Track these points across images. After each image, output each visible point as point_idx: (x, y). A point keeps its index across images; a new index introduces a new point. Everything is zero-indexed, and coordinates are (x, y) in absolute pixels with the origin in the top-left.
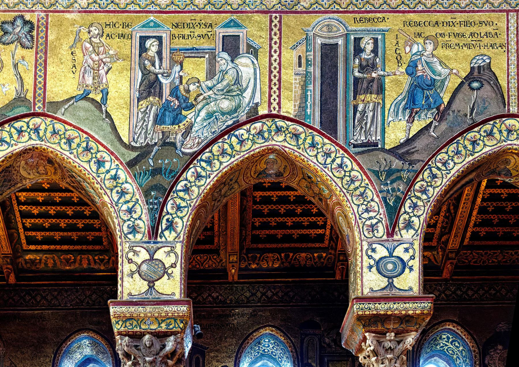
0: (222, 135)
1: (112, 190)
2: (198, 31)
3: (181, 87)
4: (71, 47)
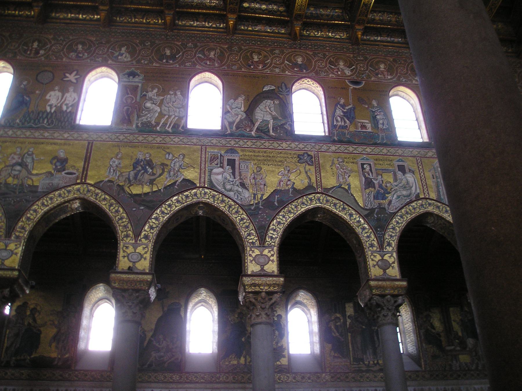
0: (405, 206)
1: (358, 227)
2: (386, 163)
3: (383, 185)
4: (331, 166)
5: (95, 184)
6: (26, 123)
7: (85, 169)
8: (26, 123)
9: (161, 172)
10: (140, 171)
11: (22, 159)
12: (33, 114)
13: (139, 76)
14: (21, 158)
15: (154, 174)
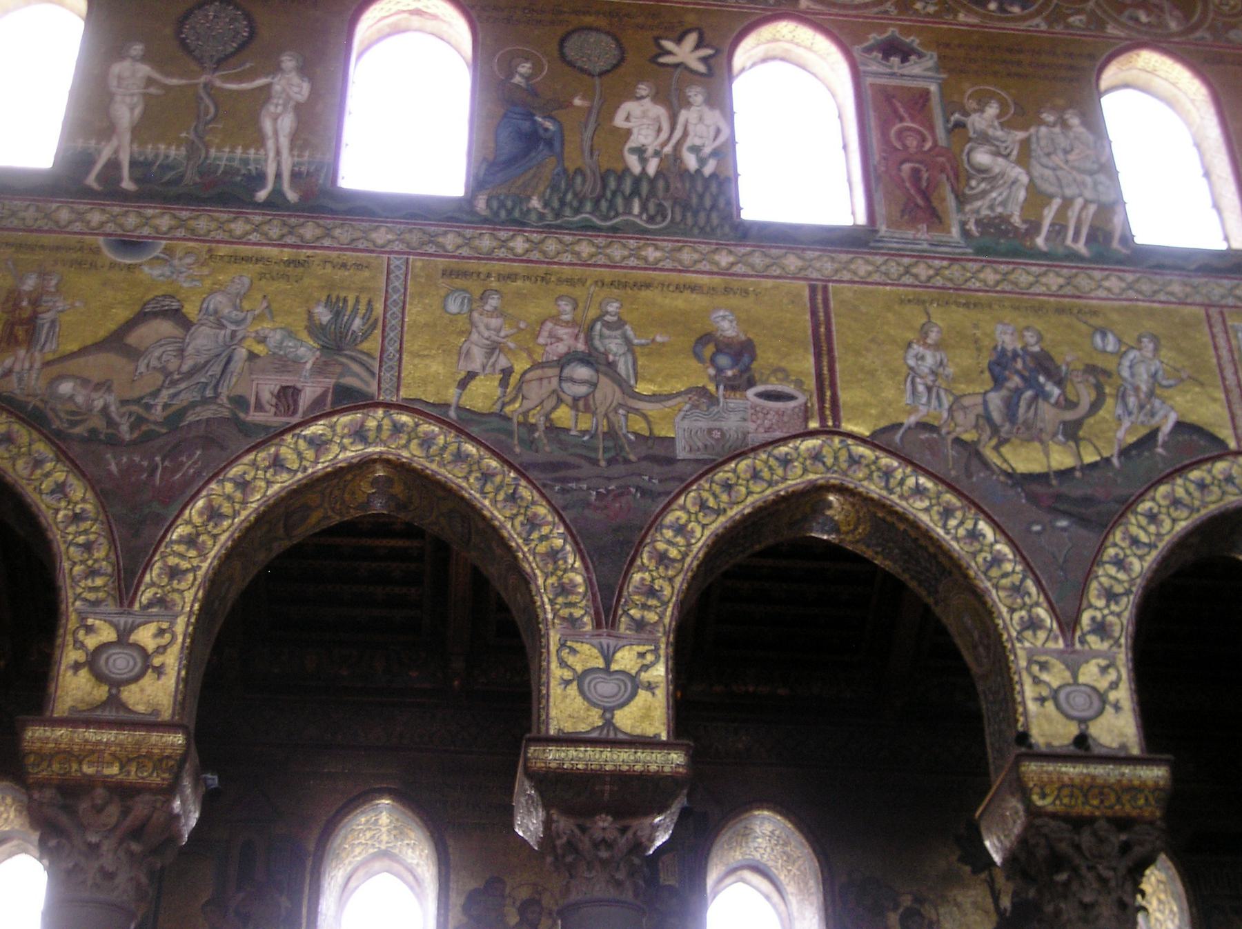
5: (874, 434)
6: (568, 212)
7: (826, 382)
8: (568, 212)
9: (1093, 396)
10: (1018, 392)
11: (589, 340)
12: (584, 181)
13: (920, 56)
14: (582, 336)
15: (1071, 405)
